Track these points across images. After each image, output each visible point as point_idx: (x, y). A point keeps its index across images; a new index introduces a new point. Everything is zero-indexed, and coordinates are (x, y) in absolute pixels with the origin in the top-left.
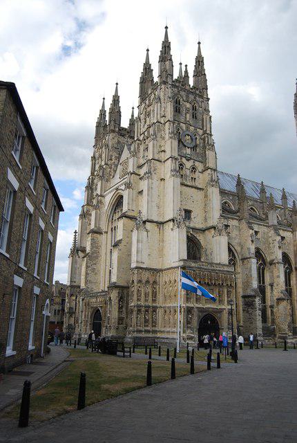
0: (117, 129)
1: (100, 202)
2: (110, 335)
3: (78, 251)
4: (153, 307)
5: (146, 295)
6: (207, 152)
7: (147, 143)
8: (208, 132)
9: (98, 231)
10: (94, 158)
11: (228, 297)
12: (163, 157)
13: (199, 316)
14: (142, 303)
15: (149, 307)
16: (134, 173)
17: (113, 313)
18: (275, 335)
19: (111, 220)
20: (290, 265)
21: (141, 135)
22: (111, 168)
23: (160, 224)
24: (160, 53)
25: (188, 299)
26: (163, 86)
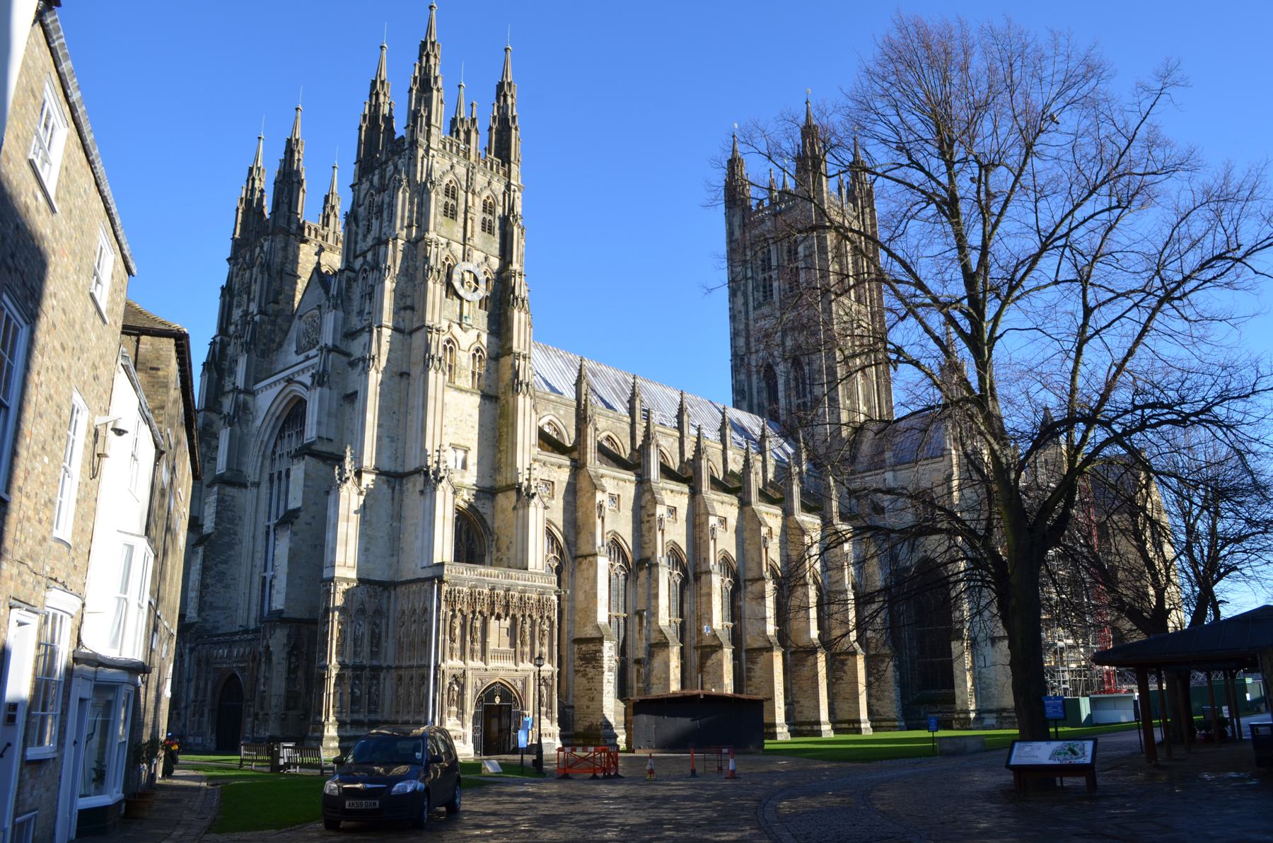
7: (370, 282)
10: (227, 291)
11: (542, 644)
15: (362, 668)
17: (276, 683)
21: (356, 257)
22: (274, 323)
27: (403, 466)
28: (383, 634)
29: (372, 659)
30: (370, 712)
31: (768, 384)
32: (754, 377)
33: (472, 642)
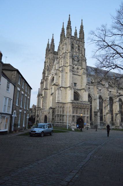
1: (47, 79)
4: (63, 115)
6: (83, 63)
8: (84, 55)
10: (45, 62)
12: (67, 65)
14: (59, 114)
16: (58, 70)
17: (50, 117)
19: (51, 85)
23: (65, 88)
24: (67, 26)
25: (73, 113)
26: (67, 39)
33: (76, 111)
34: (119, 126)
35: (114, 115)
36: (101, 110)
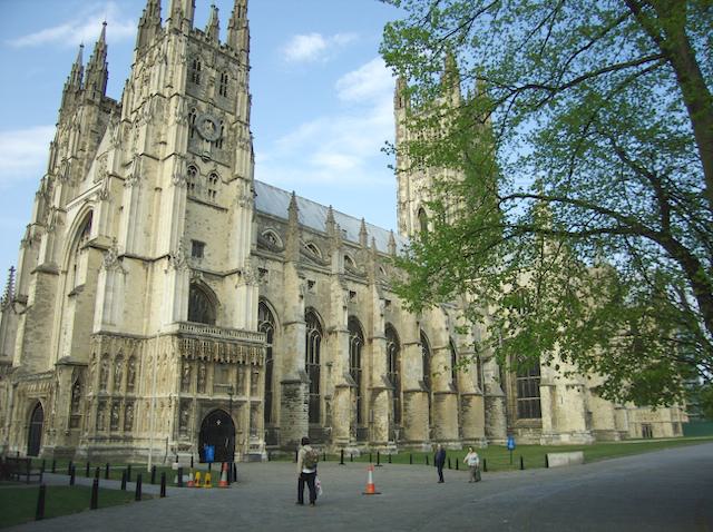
0: (98, 100)
2: (53, 446)
3: (15, 301)
5: (117, 378)
9: (52, 269)
10: (55, 145)
11: (252, 383)
13: (201, 413)
14: (109, 392)
15: (120, 398)
16: (114, 175)
17: (59, 410)
18: (331, 441)
19: (74, 251)
20: (361, 335)
21: (132, 113)
22: (81, 164)
23: (148, 262)
25: (184, 385)
26: (173, 37)
27: (154, 252)
28: (138, 370)
29: (127, 391)
30: (125, 430)
31: (421, 222)
32: (412, 215)
34: (385, 444)
35: (367, 395)
36: (313, 373)
